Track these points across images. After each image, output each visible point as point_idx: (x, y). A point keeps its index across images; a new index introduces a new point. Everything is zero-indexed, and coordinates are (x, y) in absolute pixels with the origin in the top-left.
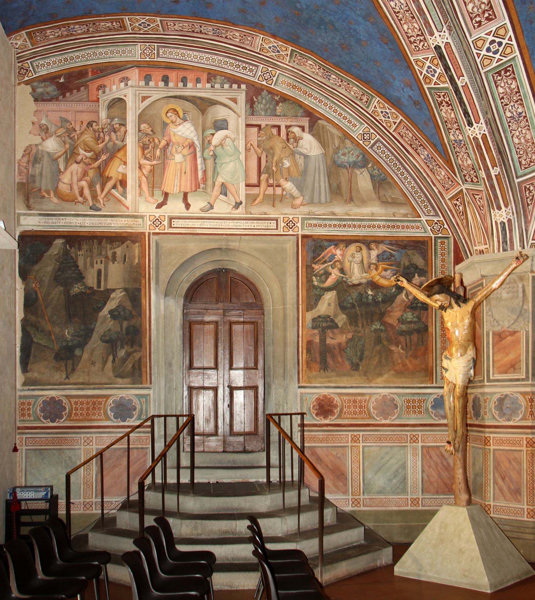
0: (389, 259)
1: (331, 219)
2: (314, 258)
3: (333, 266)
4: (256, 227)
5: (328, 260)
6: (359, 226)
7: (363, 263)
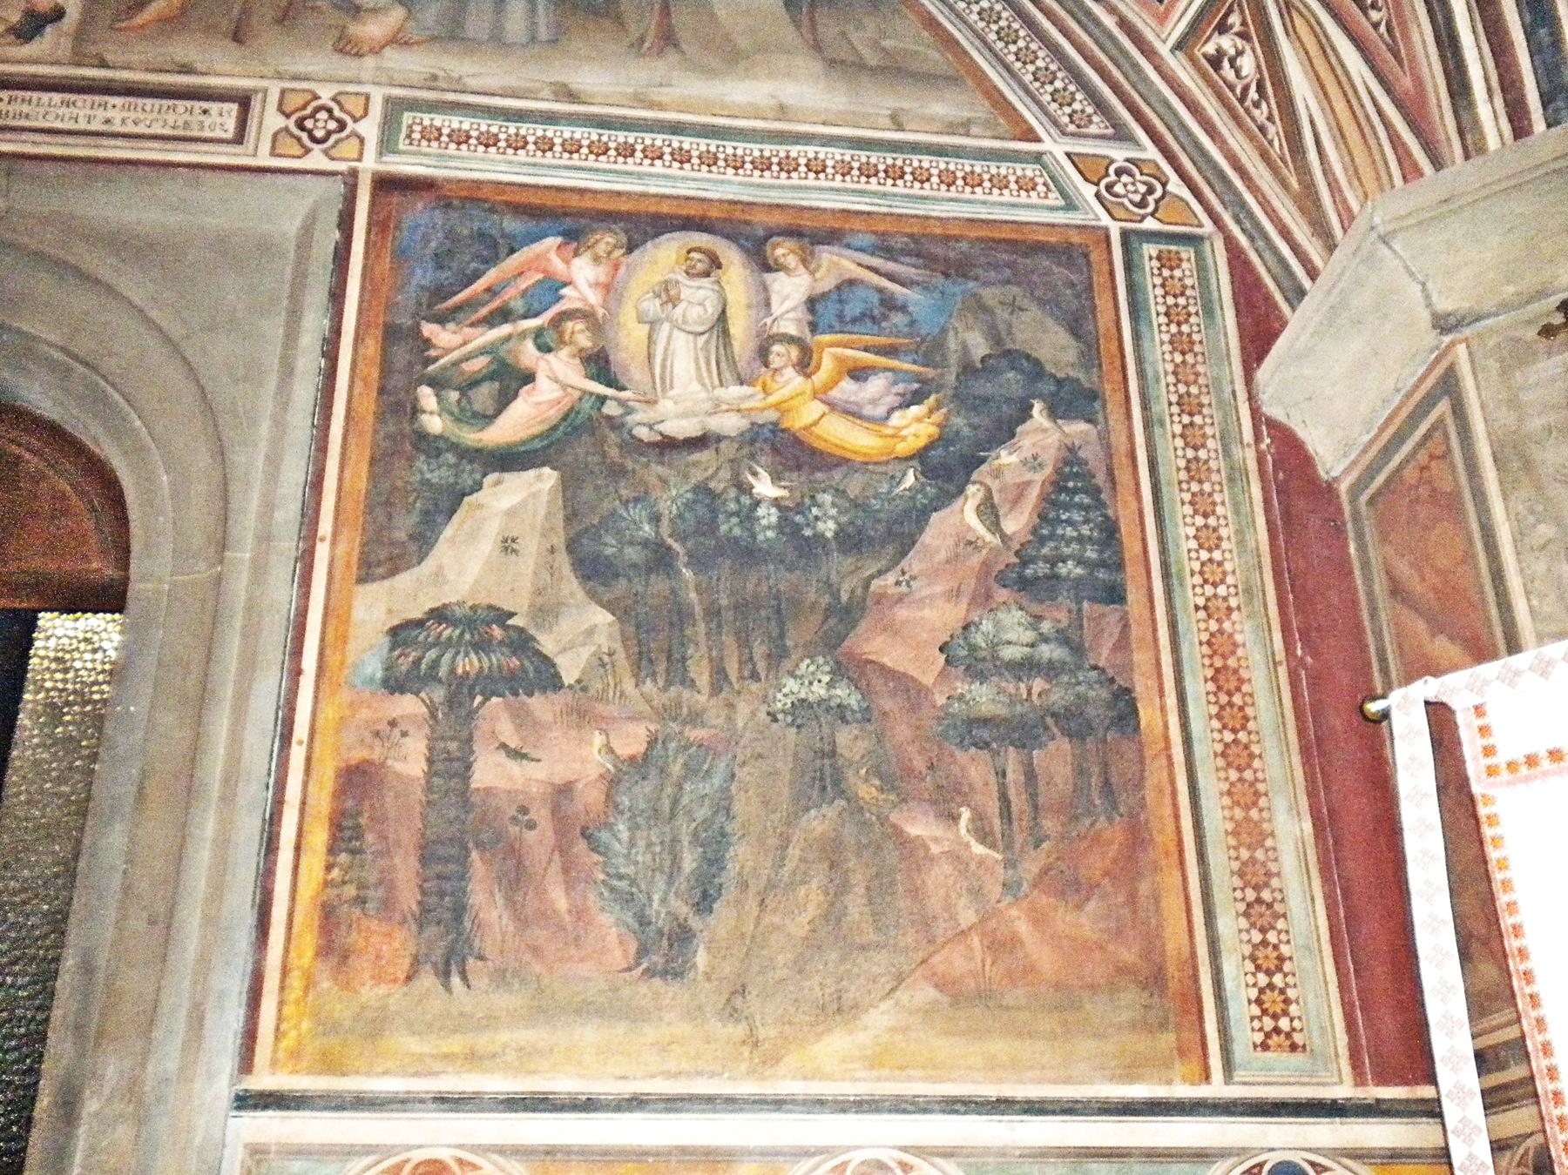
0: (873, 319)
1: (550, 118)
2: (440, 292)
3: (550, 337)
4: (117, 128)
5: (518, 305)
6: (710, 160)
7: (725, 333)
